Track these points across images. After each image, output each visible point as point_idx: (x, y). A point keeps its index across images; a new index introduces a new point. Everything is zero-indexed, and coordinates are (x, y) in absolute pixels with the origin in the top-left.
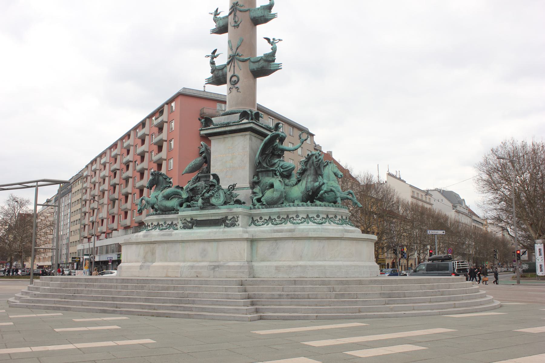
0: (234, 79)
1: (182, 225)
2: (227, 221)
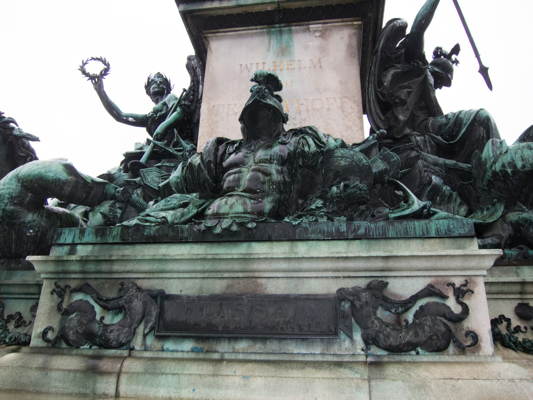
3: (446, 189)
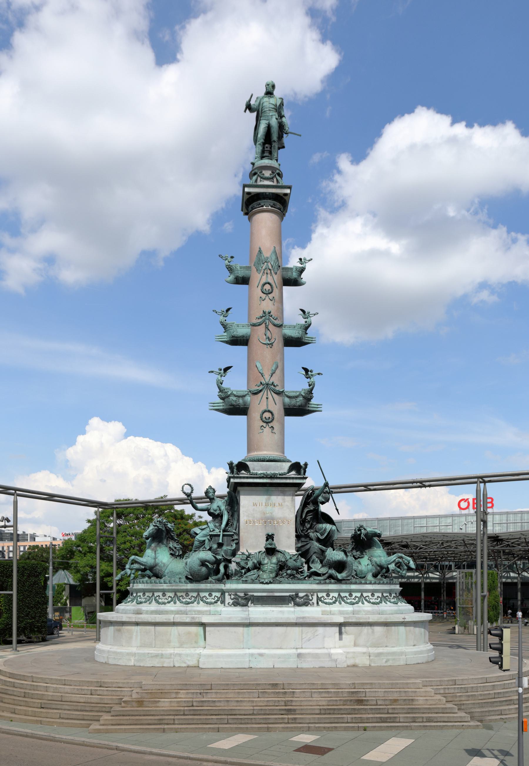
0: (267, 415)
1: (231, 601)
2: (298, 599)
3: (317, 559)
